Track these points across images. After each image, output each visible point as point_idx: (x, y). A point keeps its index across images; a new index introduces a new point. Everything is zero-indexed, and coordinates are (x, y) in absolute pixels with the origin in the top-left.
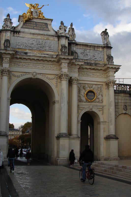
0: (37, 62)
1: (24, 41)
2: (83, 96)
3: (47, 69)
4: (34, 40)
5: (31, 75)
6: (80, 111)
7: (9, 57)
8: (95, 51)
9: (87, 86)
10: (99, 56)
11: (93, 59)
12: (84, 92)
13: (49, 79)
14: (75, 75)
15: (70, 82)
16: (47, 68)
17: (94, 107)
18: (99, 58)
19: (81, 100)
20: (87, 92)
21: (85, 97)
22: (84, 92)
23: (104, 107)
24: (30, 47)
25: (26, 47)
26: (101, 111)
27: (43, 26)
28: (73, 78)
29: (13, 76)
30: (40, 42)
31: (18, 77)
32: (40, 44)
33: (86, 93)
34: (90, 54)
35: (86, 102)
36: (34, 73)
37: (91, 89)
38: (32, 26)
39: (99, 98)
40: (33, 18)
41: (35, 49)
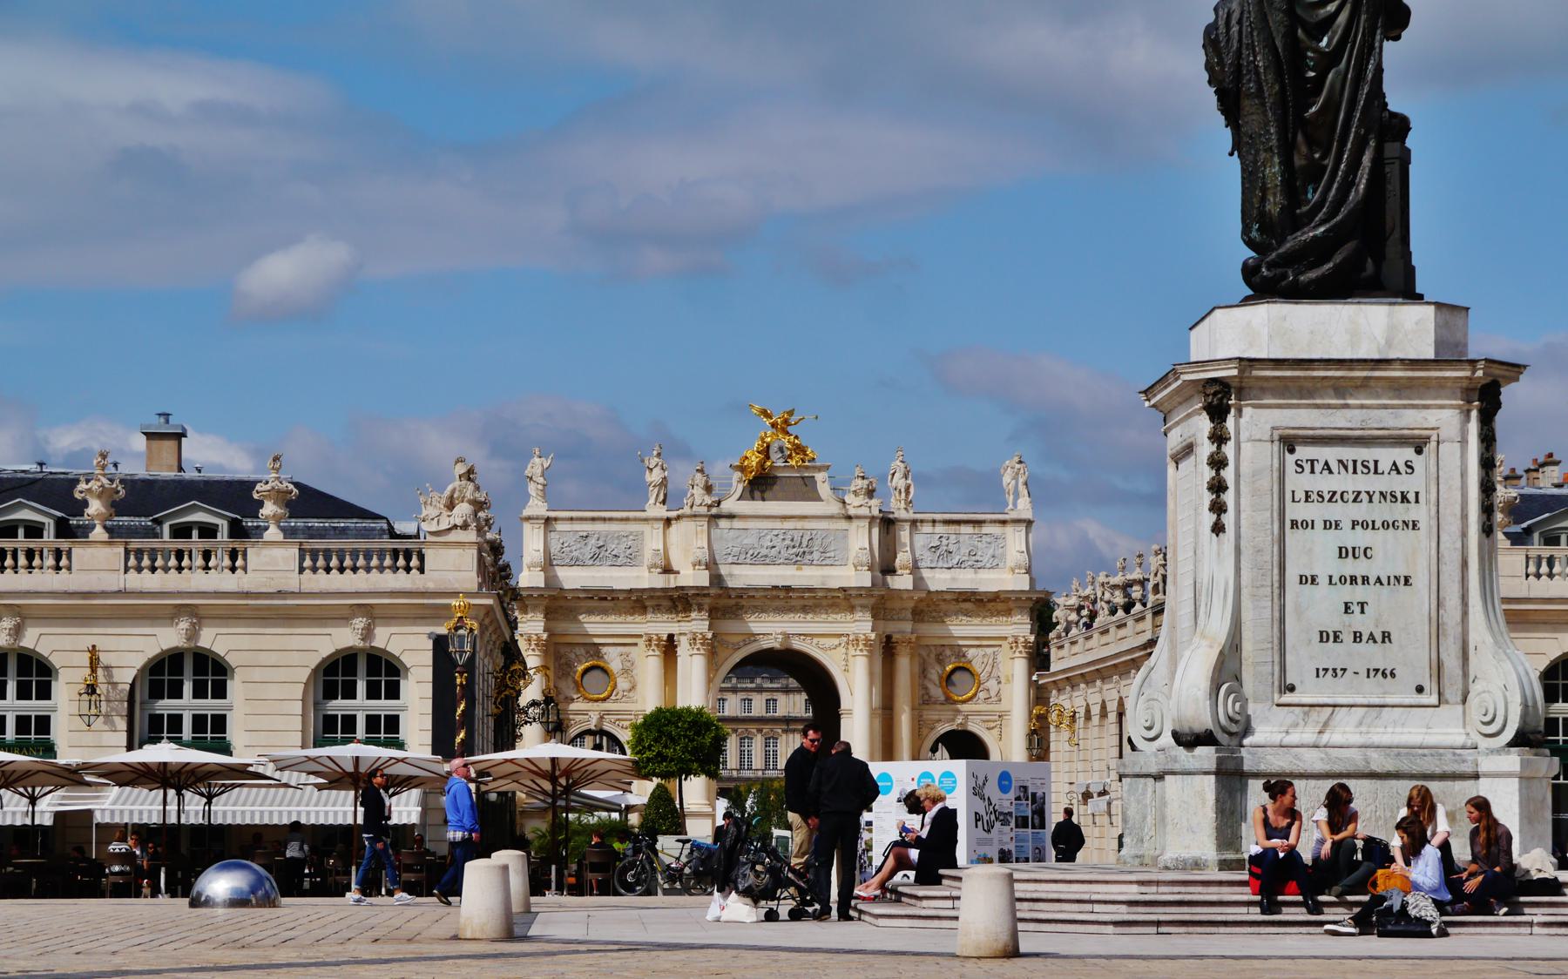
1: (745, 542)
2: (935, 684)
4: (777, 535)
6: (925, 731)
8: (975, 536)
9: (948, 652)
10: (991, 552)
11: (969, 563)
12: (940, 672)
14: (903, 628)
15: (887, 649)
17: (969, 717)
18: (988, 561)
19: (930, 697)
21: (941, 686)
22: (940, 672)
23: (1004, 717)
24: (766, 556)
26: (996, 730)
28: (894, 640)
32: (794, 547)
33: (945, 676)
34: (959, 548)
39: (988, 690)
40: (772, 467)
41: (781, 561)
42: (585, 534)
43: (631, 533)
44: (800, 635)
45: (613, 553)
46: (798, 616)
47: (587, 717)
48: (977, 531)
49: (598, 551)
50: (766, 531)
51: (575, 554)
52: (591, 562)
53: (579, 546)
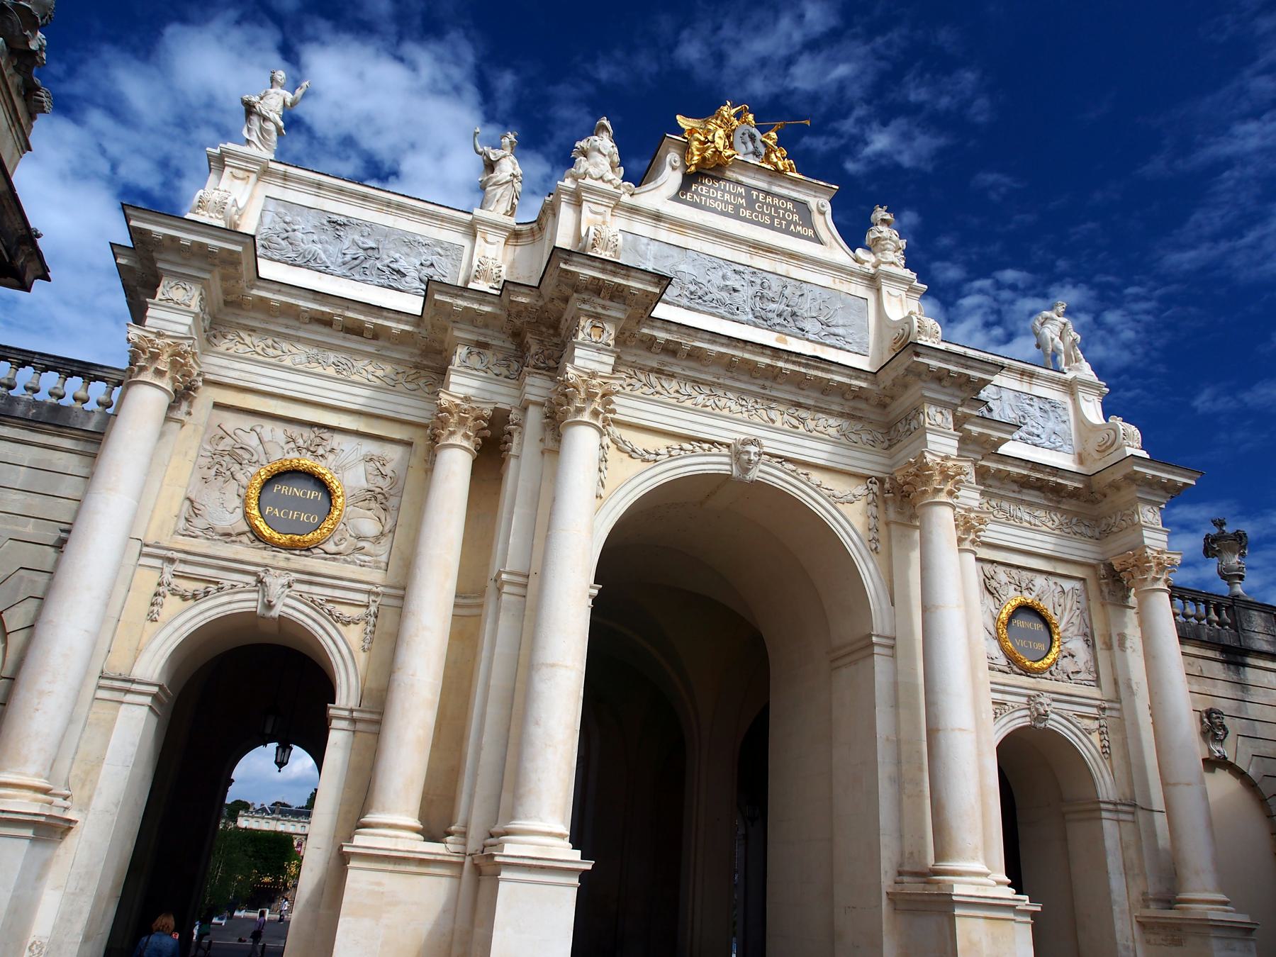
0: (764, 387)
1: (682, 267)
3: (814, 433)
5: (726, 460)
7: (619, 315)
11: (1021, 434)
13: (834, 499)
16: (821, 429)
20: (1009, 609)
24: (721, 303)
25: (700, 298)
27: (784, 214)
29: (619, 449)
30: (775, 288)
31: (650, 458)
35: (1007, 669)
36: (753, 449)
37: (1029, 598)
38: (727, 203)
39: (1073, 656)
42: (342, 220)
43: (439, 243)
44: (788, 460)
45: (394, 266)
46: (780, 417)
47: (251, 580)
48: (1024, 387)
49: (361, 253)
50: (722, 262)
51: (317, 248)
52: (344, 270)
53: (324, 237)
